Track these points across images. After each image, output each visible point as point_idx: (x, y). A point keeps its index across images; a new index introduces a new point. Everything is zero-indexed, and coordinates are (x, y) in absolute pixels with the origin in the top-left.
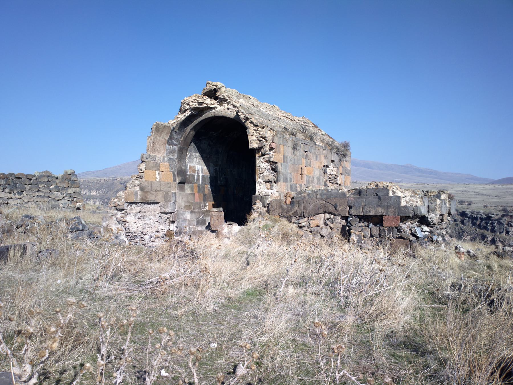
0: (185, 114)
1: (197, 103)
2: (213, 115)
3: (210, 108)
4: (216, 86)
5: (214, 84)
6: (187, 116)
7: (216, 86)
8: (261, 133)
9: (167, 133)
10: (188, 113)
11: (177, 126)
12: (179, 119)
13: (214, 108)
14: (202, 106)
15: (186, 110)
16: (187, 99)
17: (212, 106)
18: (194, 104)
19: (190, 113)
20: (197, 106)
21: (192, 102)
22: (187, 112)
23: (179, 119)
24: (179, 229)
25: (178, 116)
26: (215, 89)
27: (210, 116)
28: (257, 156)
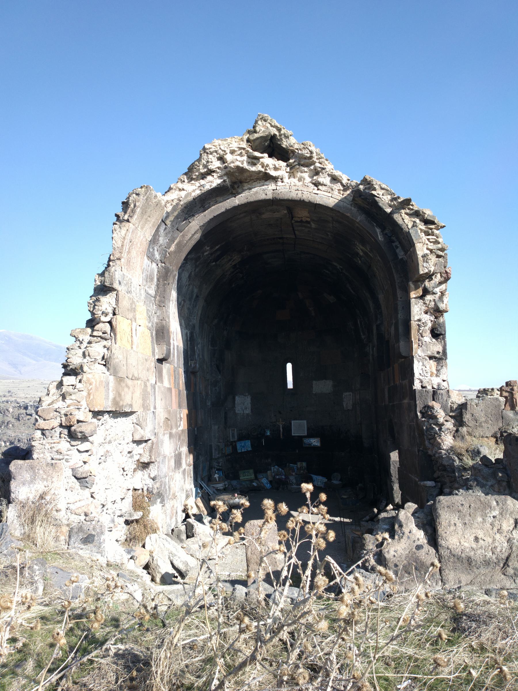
0: (202, 182)
1: (245, 158)
2: (270, 196)
3: (266, 177)
4: (279, 130)
5: (275, 122)
6: (208, 187)
7: (279, 130)
8: (440, 240)
9: (153, 225)
10: (213, 182)
11: (174, 209)
12: (183, 194)
13: (275, 179)
14: (253, 169)
15: (210, 172)
16: (217, 144)
17: (273, 173)
18: (239, 158)
19: (219, 181)
20: (245, 166)
21: (232, 152)
22: (209, 178)
23: (183, 194)
24: (158, 485)
25: (180, 185)
26: (275, 135)
27: (263, 197)
28: (413, 295)
